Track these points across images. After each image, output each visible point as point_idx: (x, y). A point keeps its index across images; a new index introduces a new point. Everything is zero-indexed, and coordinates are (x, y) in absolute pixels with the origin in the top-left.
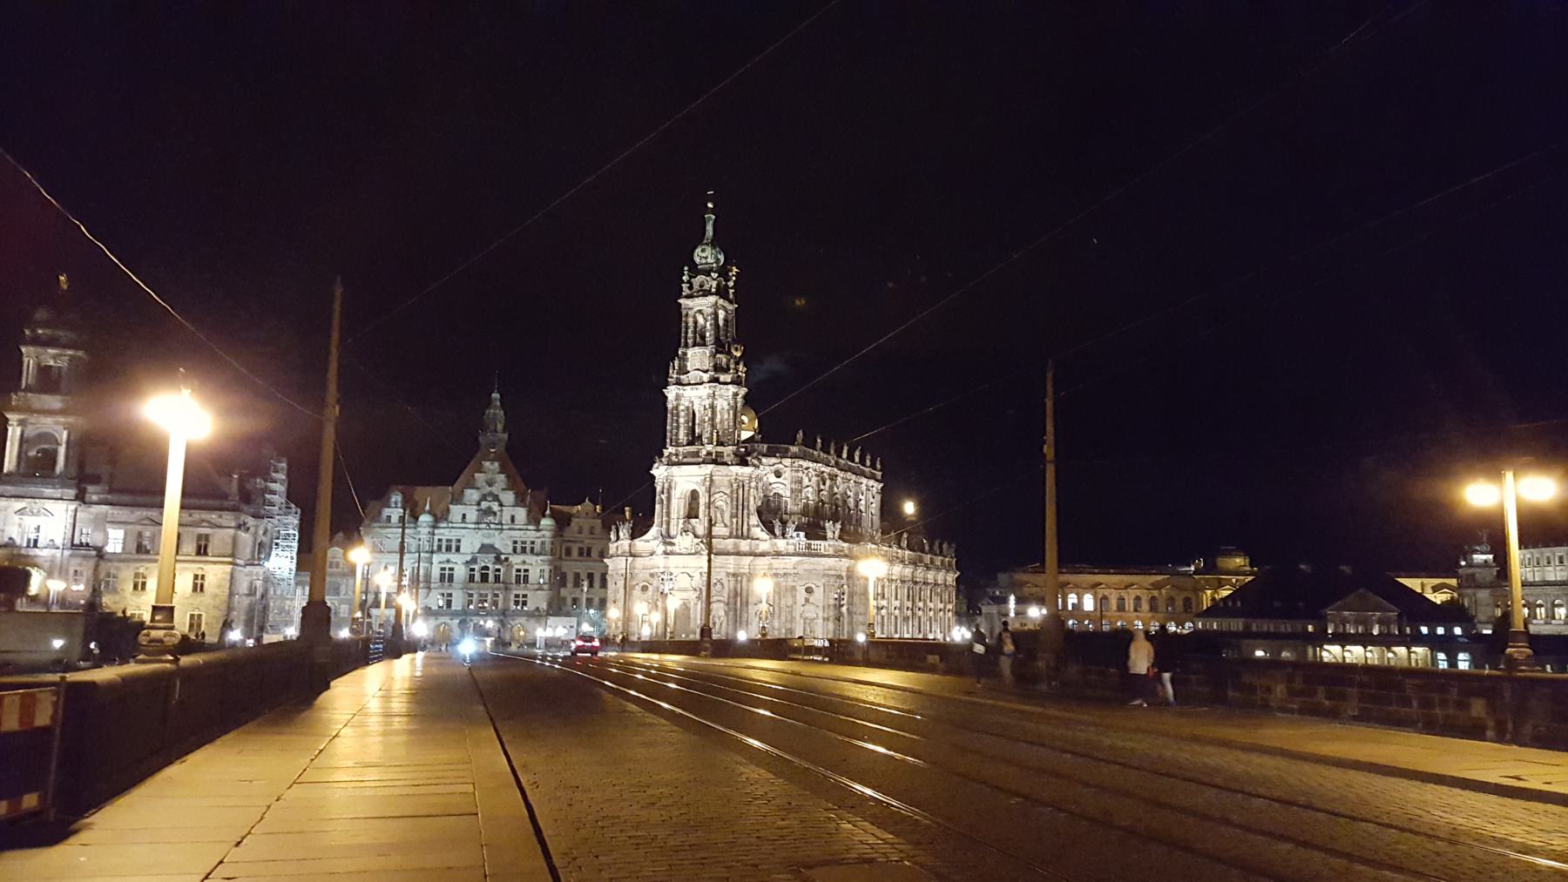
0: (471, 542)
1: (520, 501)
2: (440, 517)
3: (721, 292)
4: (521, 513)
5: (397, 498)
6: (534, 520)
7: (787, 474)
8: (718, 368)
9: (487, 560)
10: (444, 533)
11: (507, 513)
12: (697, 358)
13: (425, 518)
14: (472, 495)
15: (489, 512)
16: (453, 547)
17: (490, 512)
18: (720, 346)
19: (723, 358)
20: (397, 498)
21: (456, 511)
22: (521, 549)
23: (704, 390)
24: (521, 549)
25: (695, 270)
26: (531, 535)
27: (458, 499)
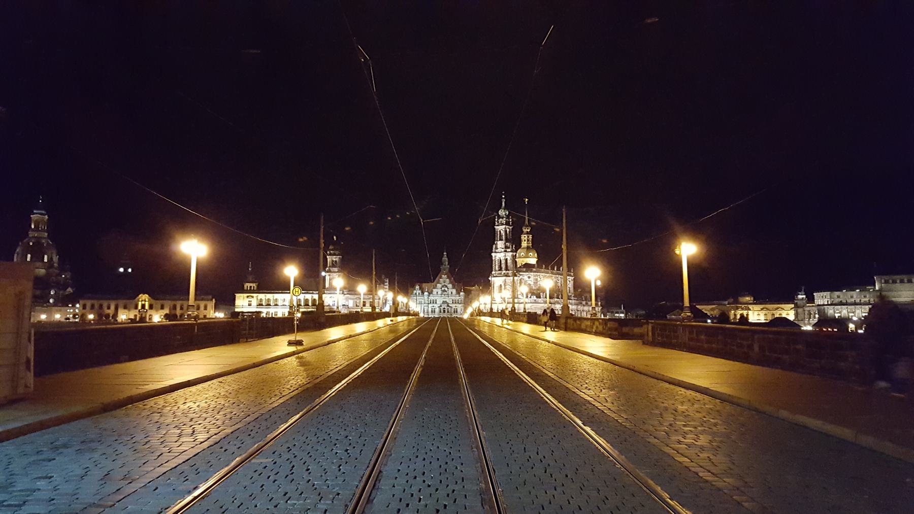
0: (439, 302)
1: (454, 287)
2: (430, 293)
3: (507, 223)
4: (454, 291)
5: (417, 287)
6: (458, 293)
7: (532, 279)
8: (506, 247)
9: (445, 306)
10: (431, 298)
11: (450, 291)
12: (500, 244)
13: (426, 293)
14: (439, 286)
15: (445, 291)
16: (435, 302)
17: (445, 291)
18: (507, 240)
19: (508, 244)
20: (417, 287)
21: (435, 291)
22: (454, 302)
23: (503, 254)
24: (454, 302)
25: (499, 217)
26: (458, 298)
27: (435, 287)
